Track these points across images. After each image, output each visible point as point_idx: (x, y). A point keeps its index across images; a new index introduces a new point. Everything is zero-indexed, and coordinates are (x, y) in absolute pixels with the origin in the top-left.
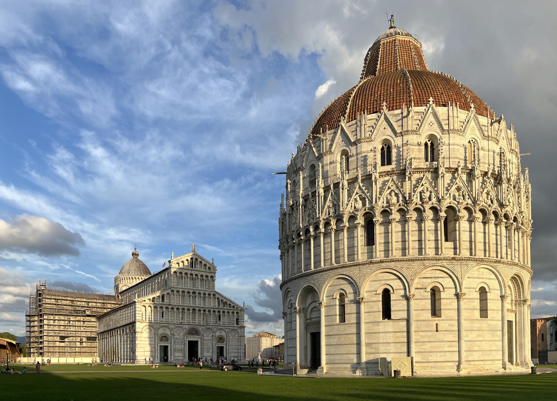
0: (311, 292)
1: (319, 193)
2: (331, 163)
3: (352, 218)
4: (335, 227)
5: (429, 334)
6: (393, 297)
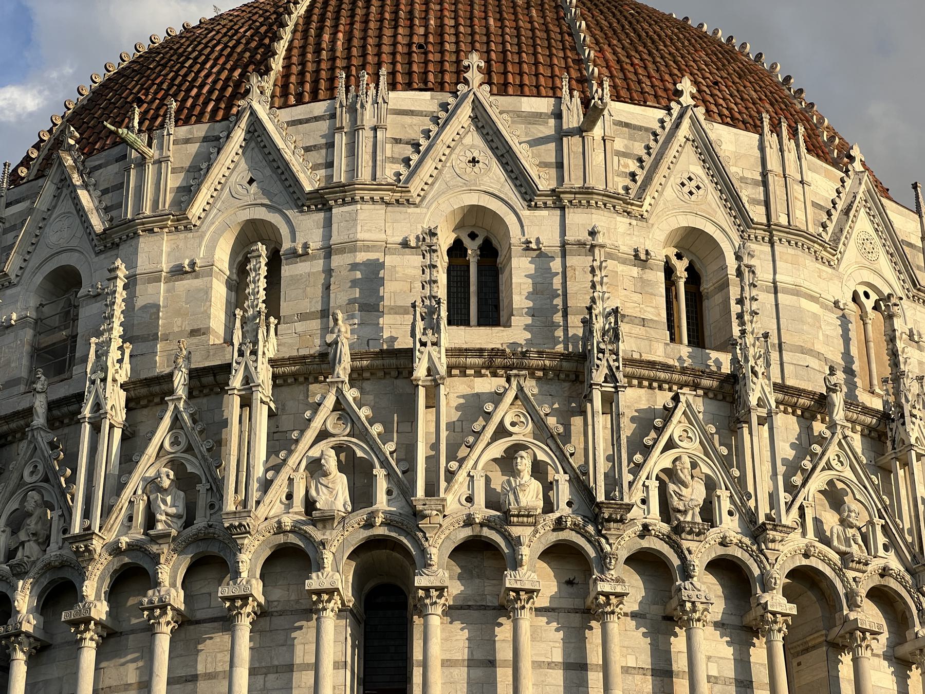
1: (97, 406)
3: (291, 558)
4: (177, 598)
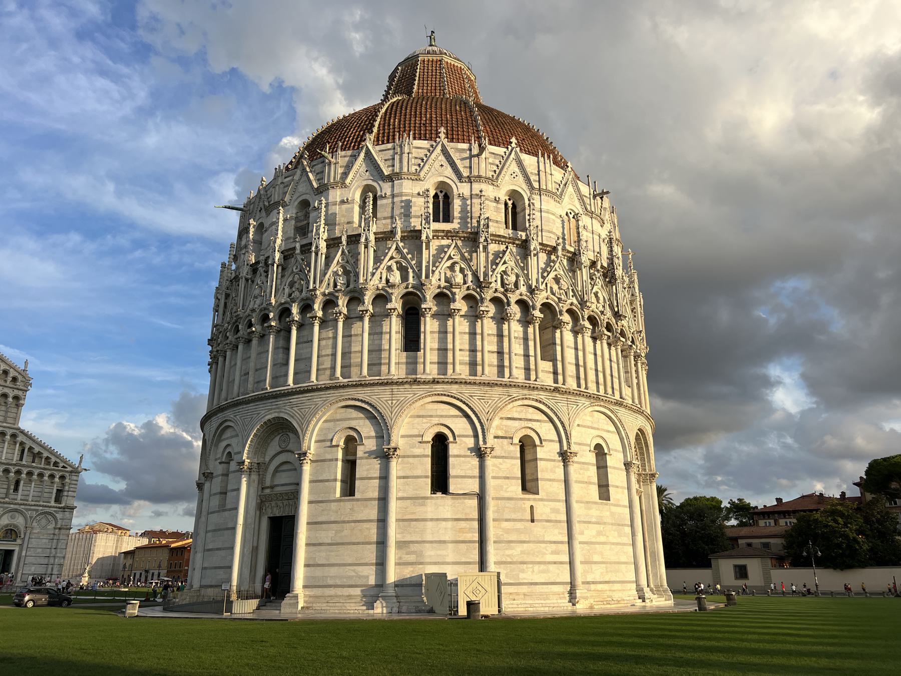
0: (283, 431)
1: (317, 247)
2: (343, 202)
3: (381, 298)
4: (345, 310)
5: (519, 525)
6: (453, 449)
